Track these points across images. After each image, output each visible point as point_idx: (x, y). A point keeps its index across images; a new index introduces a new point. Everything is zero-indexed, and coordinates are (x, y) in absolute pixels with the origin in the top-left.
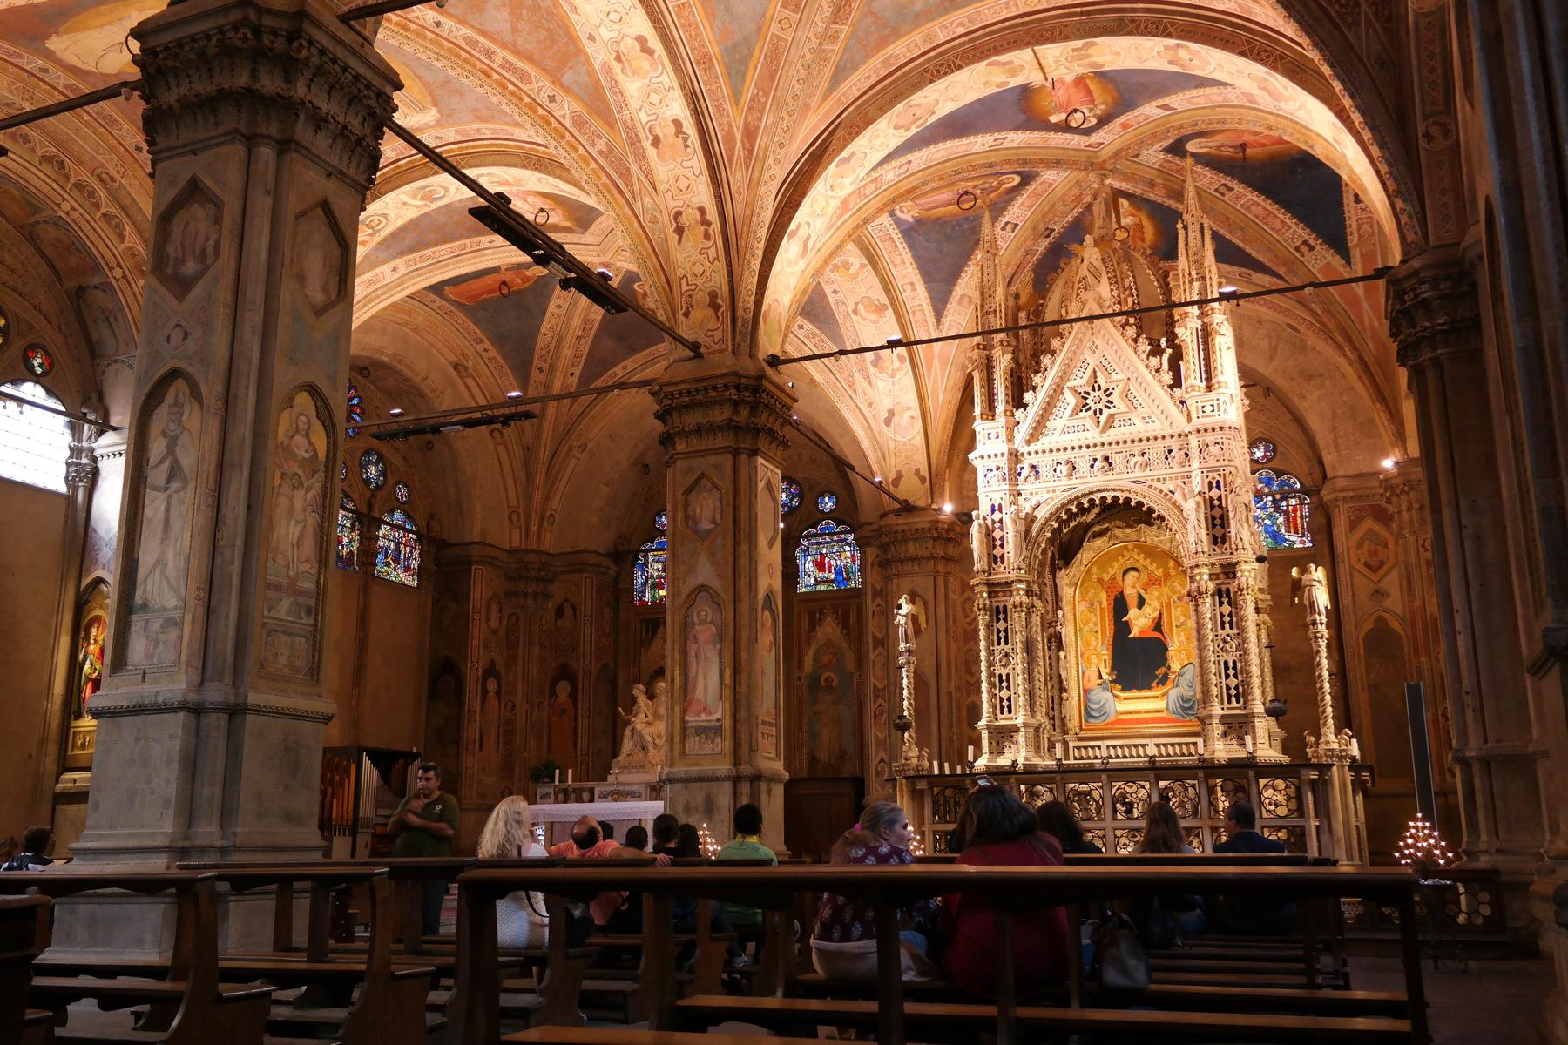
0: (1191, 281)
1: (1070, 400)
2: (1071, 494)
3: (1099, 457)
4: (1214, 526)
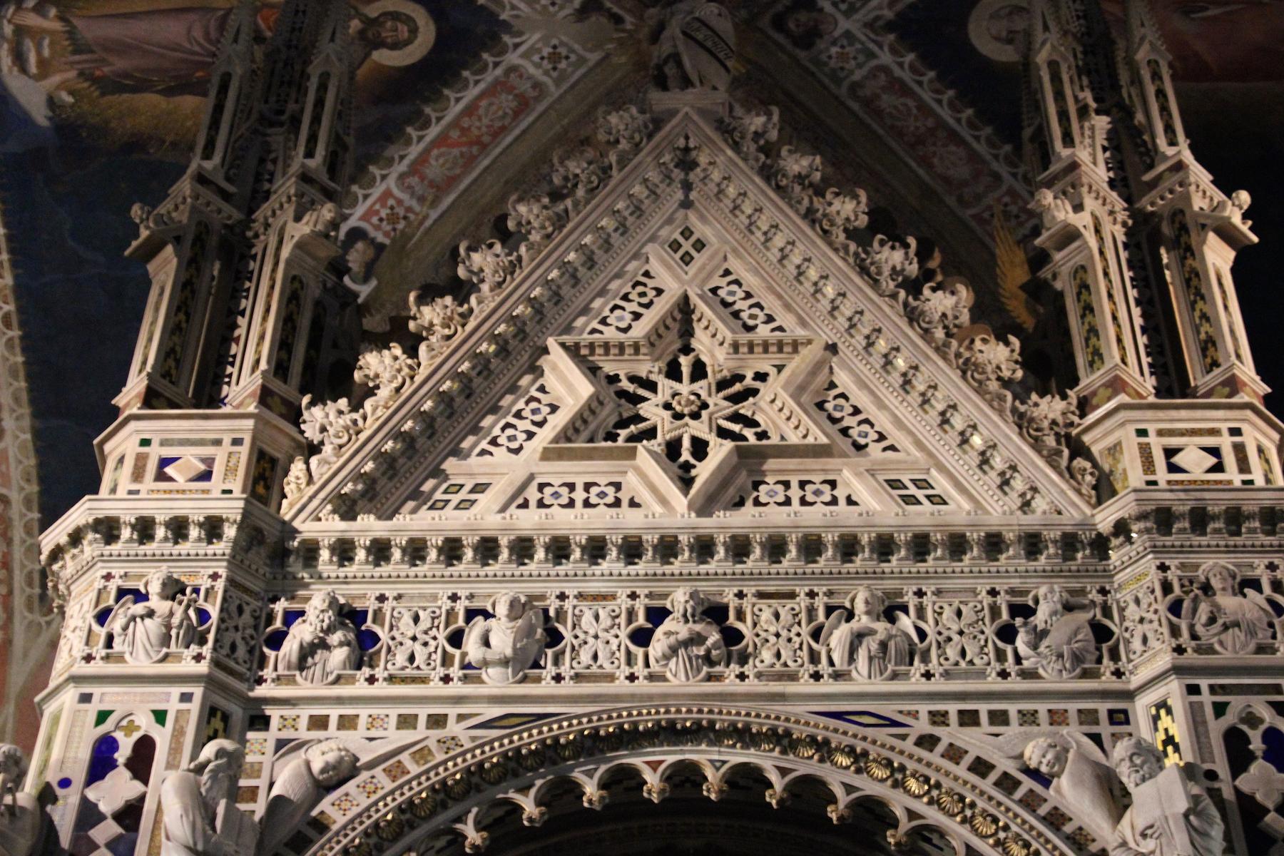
0: (1083, 112)
1: (567, 386)
2: (529, 739)
3: (679, 598)
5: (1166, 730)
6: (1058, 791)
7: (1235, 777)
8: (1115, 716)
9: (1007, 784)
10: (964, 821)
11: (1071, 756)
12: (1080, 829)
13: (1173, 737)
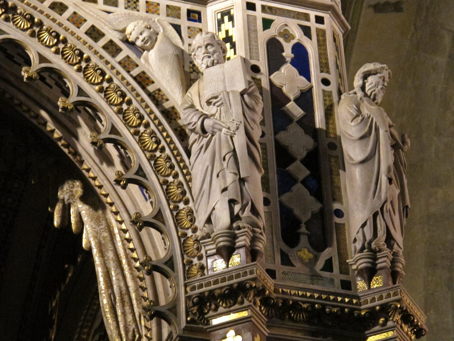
4: (286, 182)
5: (227, 32)
6: (147, 60)
7: (270, 73)
8: (191, 14)
9: (112, 48)
10: (79, 70)
11: (160, 37)
12: (159, 90)
13: (231, 38)
